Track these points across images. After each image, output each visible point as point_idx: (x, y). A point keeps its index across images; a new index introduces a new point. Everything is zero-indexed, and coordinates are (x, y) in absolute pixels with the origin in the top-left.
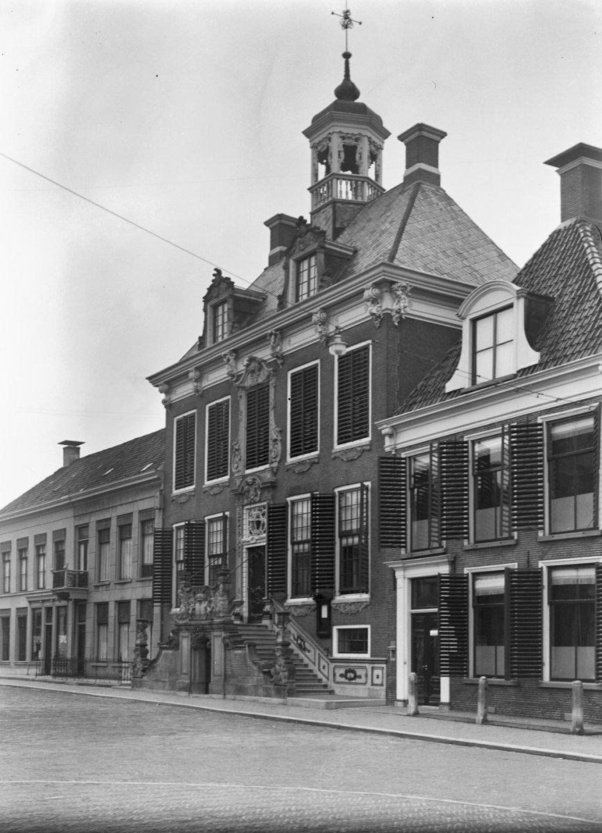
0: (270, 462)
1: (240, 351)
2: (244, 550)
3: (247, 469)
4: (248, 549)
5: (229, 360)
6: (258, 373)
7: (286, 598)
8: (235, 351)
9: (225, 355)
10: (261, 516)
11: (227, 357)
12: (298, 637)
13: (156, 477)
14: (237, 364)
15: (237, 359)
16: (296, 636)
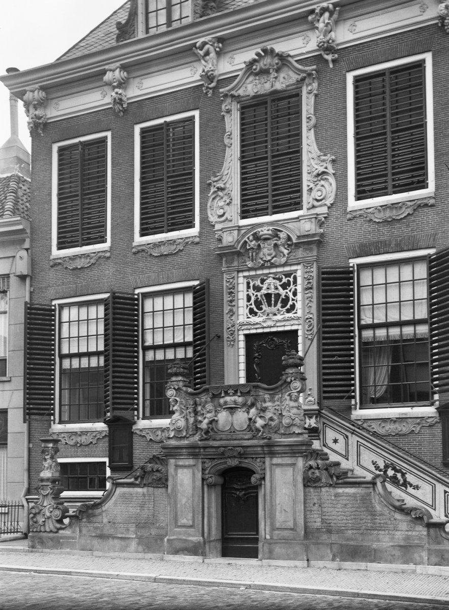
0: (305, 205)
1: (228, 42)
2: (242, 338)
3: (243, 218)
4: (246, 336)
5: (207, 53)
6: (274, 74)
7: (349, 409)
8: (220, 40)
9: (205, 44)
10: (280, 288)
11: (207, 46)
12: (387, 467)
13: (20, 227)
14: (217, 62)
15: (219, 54)
16: (382, 466)
